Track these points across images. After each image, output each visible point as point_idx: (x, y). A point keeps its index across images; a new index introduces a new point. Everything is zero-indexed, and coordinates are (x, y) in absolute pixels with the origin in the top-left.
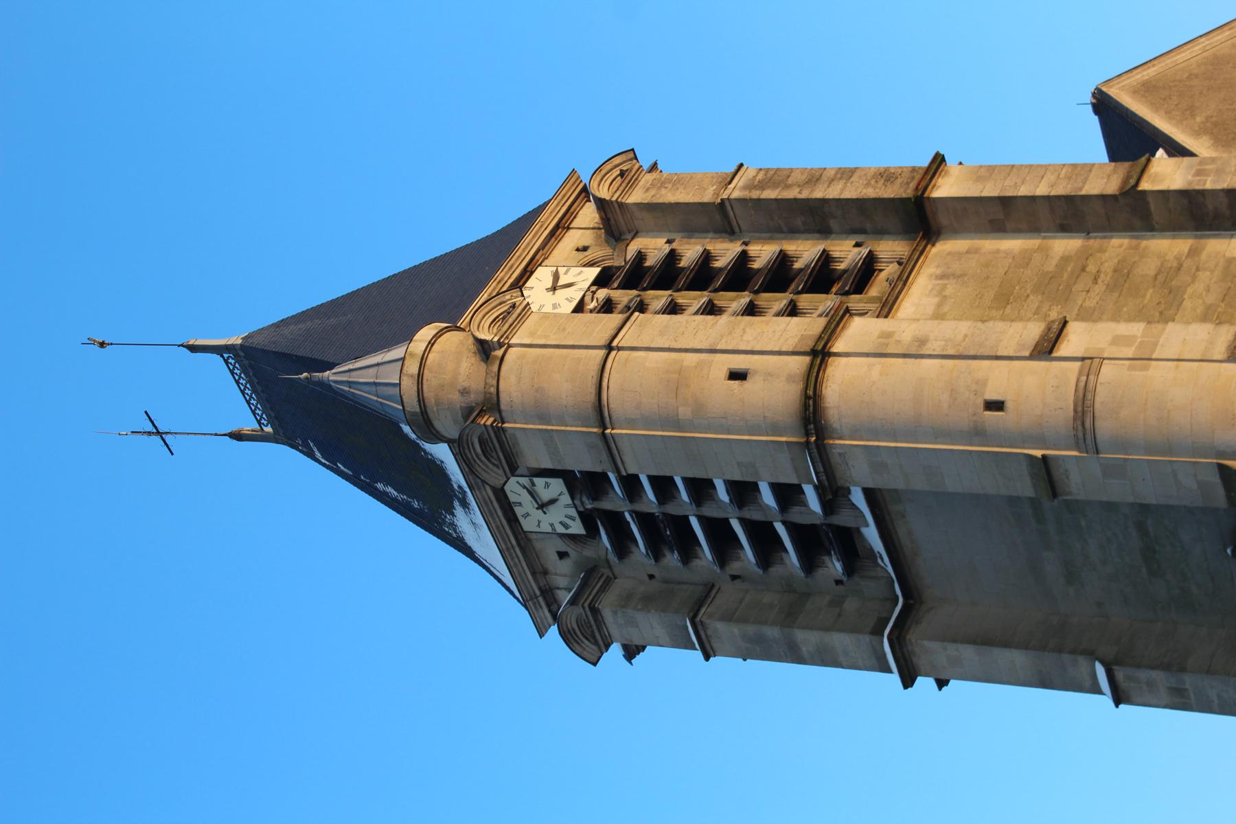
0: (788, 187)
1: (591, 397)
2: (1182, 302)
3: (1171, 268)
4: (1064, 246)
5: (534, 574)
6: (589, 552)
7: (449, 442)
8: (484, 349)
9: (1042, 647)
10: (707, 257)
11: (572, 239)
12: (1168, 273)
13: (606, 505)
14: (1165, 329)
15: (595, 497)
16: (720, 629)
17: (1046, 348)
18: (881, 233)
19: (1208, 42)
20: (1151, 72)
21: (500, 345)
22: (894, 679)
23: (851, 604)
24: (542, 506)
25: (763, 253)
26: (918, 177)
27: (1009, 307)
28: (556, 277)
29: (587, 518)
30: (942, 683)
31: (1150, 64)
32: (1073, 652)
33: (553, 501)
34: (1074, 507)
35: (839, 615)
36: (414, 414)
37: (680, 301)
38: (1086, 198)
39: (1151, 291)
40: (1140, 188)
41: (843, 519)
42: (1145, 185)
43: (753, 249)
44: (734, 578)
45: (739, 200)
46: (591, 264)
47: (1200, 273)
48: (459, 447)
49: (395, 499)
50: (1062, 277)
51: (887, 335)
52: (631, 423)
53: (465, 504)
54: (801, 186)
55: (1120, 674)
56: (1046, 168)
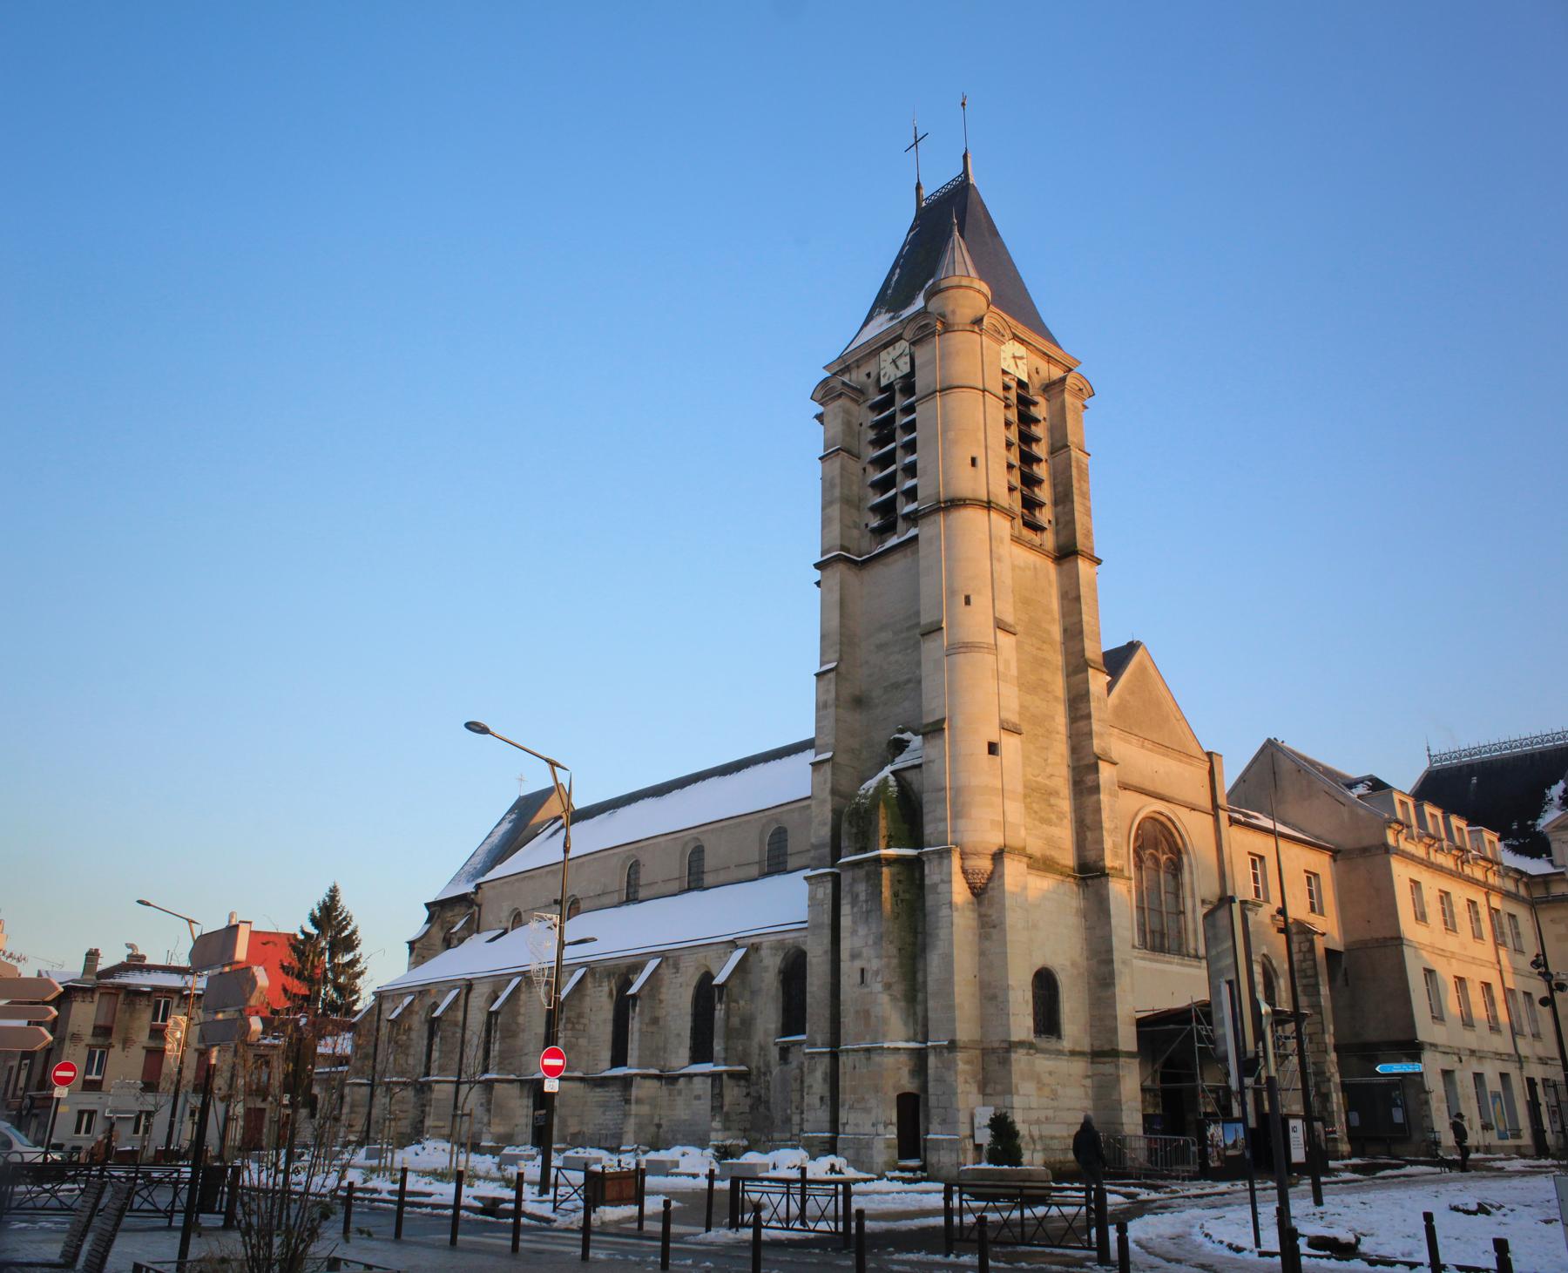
0: (1079, 481)
1: (956, 384)
4: (1056, 632)
5: (857, 361)
6: (872, 390)
7: (925, 306)
8: (978, 321)
9: (841, 635)
10: (1037, 440)
11: (1043, 365)
13: (898, 396)
15: (901, 390)
16: (836, 463)
17: (1000, 625)
18: (1057, 533)
20: (1151, 670)
21: (981, 330)
22: (819, 559)
23: (855, 533)
24: (894, 361)
25: (1041, 471)
26: (1089, 551)
28: (1021, 358)
29: (890, 387)
30: (818, 584)
32: (841, 650)
33: (897, 367)
34: (917, 646)
35: (849, 527)
36: (939, 286)
37: (1012, 427)
38: (1082, 640)
41: (901, 525)
42: (1090, 671)
43: (1043, 465)
44: (864, 469)
45: (1070, 458)
46: (1029, 377)
48: (923, 312)
49: (891, 280)
51: (1002, 541)
52: (943, 406)
53: (892, 319)
54: (1080, 489)
55: (832, 675)
56: (1097, 619)
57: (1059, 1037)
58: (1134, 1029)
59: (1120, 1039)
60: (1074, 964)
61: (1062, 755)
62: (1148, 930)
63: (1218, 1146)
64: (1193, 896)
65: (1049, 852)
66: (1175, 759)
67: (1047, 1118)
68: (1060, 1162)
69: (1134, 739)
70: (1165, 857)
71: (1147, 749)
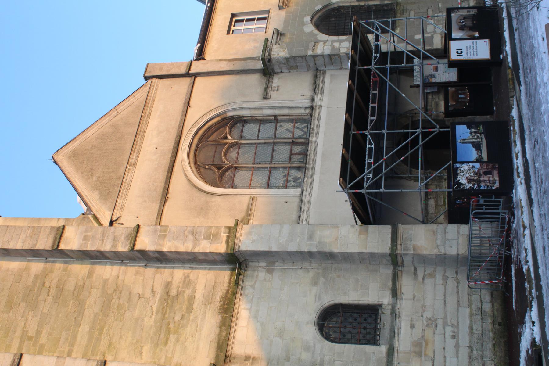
2: (84, 311)
3: (80, 285)
12: (79, 289)
14: (64, 363)
19: (100, 124)
27: (11, 311)
31: (75, 140)
39: (71, 302)
40: (60, 248)
47: (92, 290)
50: (34, 291)
57: (380, 305)
58: (371, 228)
59: (380, 251)
60: (315, 283)
61: (137, 273)
62: (289, 165)
63: (478, 174)
64: (261, 108)
65: (217, 304)
66: (147, 124)
67: (454, 337)
68: (493, 323)
69: (128, 177)
70: (229, 137)
71: (137, 158)
